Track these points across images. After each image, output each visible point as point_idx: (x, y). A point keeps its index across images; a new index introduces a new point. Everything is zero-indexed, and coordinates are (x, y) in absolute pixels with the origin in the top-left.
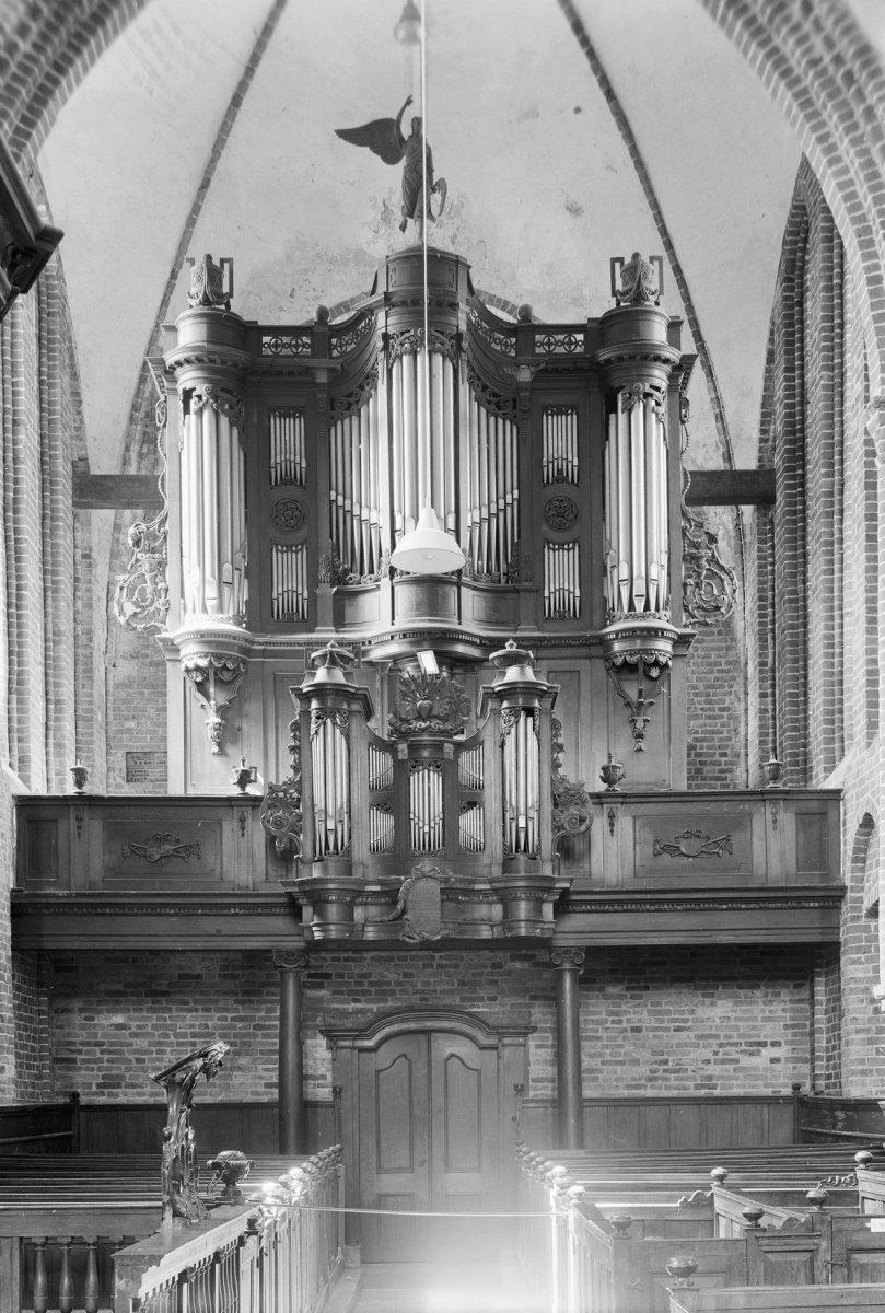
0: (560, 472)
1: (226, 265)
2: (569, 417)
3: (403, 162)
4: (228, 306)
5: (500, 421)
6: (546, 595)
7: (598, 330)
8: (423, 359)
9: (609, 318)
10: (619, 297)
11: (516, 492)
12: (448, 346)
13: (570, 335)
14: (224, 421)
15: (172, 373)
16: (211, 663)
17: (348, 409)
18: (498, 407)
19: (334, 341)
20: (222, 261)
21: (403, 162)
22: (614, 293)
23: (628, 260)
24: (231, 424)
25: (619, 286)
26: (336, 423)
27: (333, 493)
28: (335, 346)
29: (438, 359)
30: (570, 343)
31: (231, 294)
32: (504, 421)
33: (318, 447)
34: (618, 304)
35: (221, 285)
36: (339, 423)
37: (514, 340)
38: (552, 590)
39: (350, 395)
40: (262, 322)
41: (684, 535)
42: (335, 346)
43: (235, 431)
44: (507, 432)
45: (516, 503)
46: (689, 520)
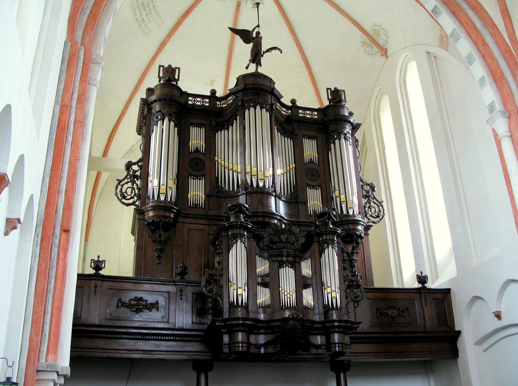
0: (311, 159)
1: (177, 70)
2: (313, 141)
3: (251, 45)
4: (177, 83)
5: (286, 138)
6: (309, 206)
7: (322, 111)
8: (258, 108)
9: (327, 107)
10: (331, 100)
11: (294, 165)
12: (268, 107)
13: (312, 112)
14: (172, 124)
15: (150, 105)
16: (161, 220)
17: (224, 126)
18: (285, 132)
19: (218, 103)
20: (176, 68)
21: (251, 45)
22: (328, 99)
23: (333, 89)
24: (175, 126)
25: (330, 97)
26: (218, 132)
27: (216, 158)
28: (218, 105)
29: (264, 110)
30: (312, 115)
31: (178, 80)
32: (288, 139)
33: (210, 142)
34: (330, 103)
35: (175, 75)
36: (219, 132)
37: (290, 111)
38: (311, 204)
39: (225, 121)
40: (189, 92)
41: (362, 188)
42: (218, 105)
43: (176, 129)
44: (289, 143)
45: (294, 169)
46: (363, 182)
